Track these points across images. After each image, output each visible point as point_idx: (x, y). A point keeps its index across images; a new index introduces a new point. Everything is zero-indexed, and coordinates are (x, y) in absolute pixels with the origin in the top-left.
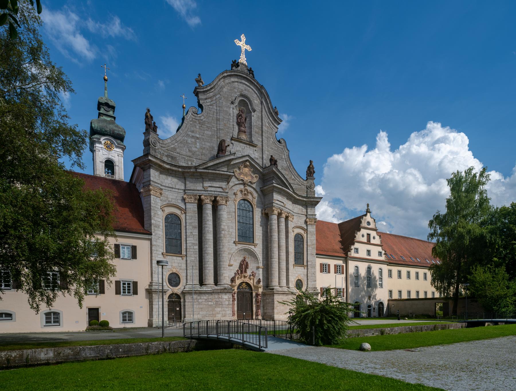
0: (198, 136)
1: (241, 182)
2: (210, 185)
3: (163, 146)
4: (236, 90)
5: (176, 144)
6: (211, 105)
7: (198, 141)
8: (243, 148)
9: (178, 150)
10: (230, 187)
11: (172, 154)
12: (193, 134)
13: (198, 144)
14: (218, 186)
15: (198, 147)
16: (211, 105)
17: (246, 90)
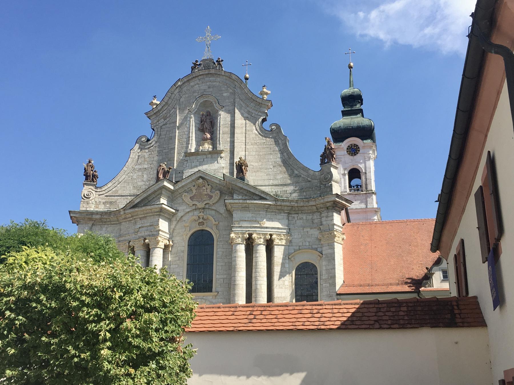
0: (146, 166)
1: (194, 207)
2: (140, 226)
3: (101, 193)
4: (195, 94)
5: (119, 185)
6: (164, 125)
7: (145, 172)
8: (202, 160)
9: (120, 192)
10: (178, 219)
11: (111, 199)
12: (140, 167)
13: (145, 176)
14: (148, 224)
15: (145, 180)
16: (164, 125)
17: (209, 87)
